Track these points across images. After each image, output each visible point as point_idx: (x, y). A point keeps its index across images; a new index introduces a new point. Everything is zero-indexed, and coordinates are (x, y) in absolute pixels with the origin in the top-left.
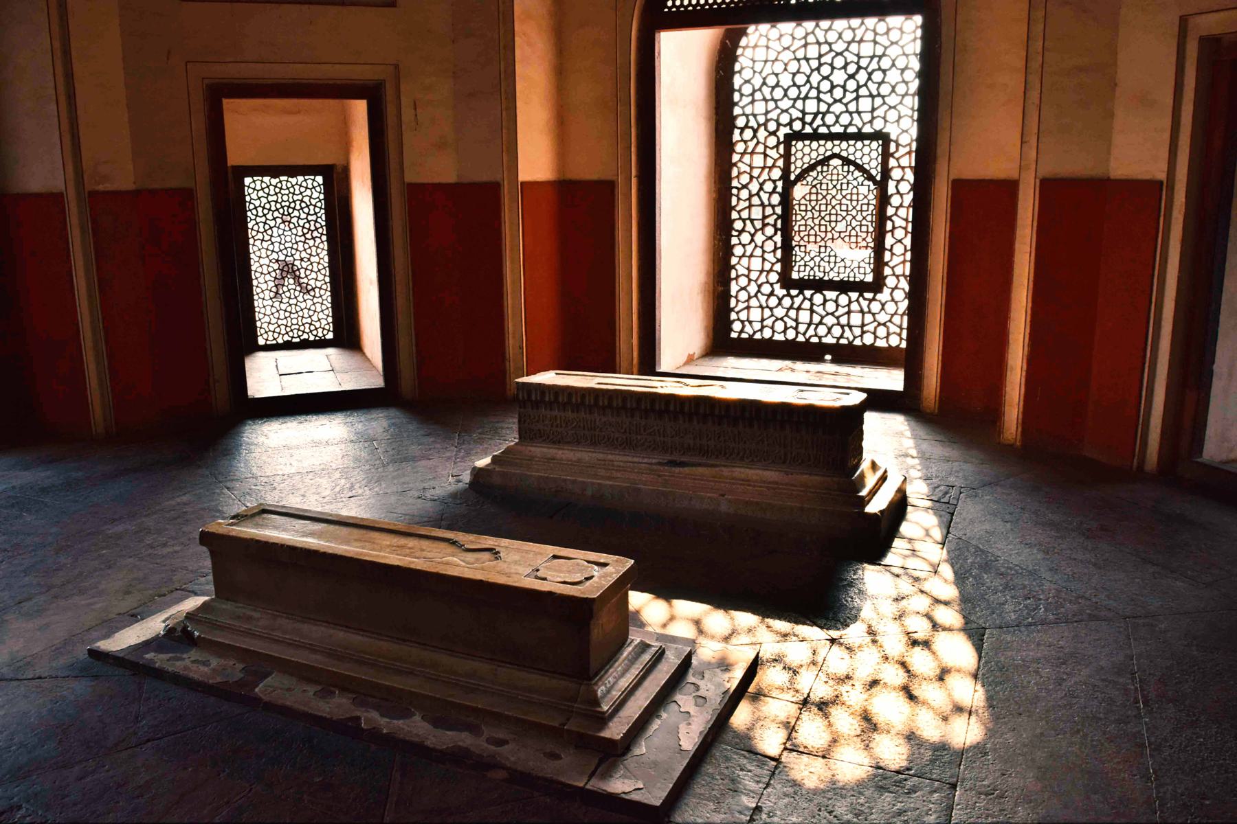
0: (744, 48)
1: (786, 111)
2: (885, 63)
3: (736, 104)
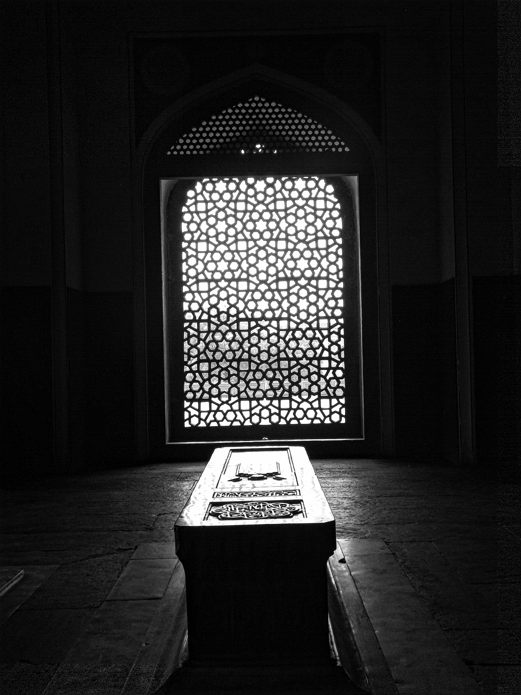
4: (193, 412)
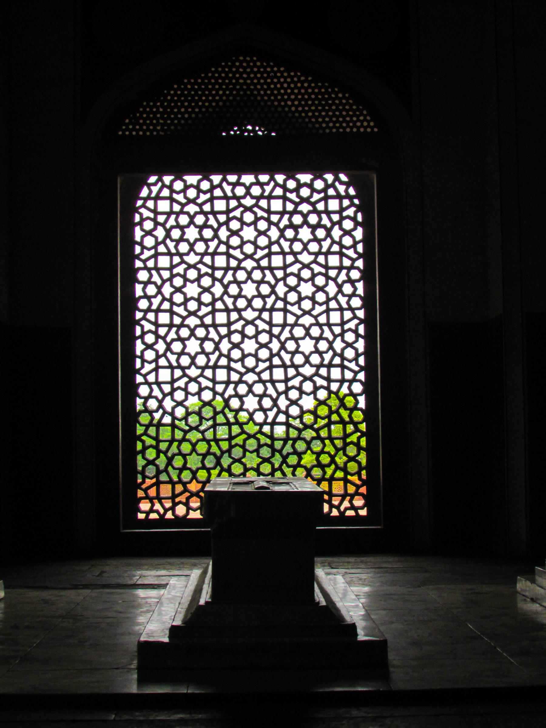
0: (146, 199)
1: (194, 266)
2: (297, 220)
3: (138, 257)
4: (149, 441)
